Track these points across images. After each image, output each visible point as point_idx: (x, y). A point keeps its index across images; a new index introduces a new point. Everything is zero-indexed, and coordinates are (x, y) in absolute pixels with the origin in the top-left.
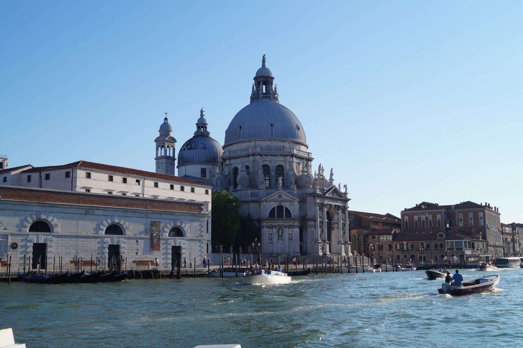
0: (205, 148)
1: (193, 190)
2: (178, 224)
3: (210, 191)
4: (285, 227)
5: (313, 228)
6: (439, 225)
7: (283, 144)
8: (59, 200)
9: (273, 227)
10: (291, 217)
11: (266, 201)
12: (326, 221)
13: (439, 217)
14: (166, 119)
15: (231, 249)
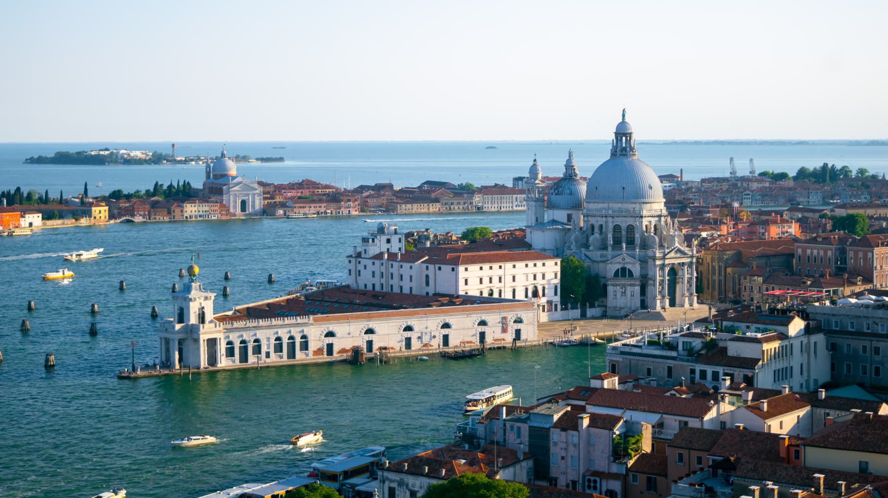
0: (571, 194)
1: (544, 264)
2: (519, 316)
3: (559, 261)
4: (628, 285)
5: (652, 287)
6: (830, 263)
7: (634, 206)
8: (453, 312)
9: (617, 285)
10: (633, 276)
11: (611, 263)
12: (667, 278)
13: (829, 253)
14: (535, 160)
15: (579, 305)
